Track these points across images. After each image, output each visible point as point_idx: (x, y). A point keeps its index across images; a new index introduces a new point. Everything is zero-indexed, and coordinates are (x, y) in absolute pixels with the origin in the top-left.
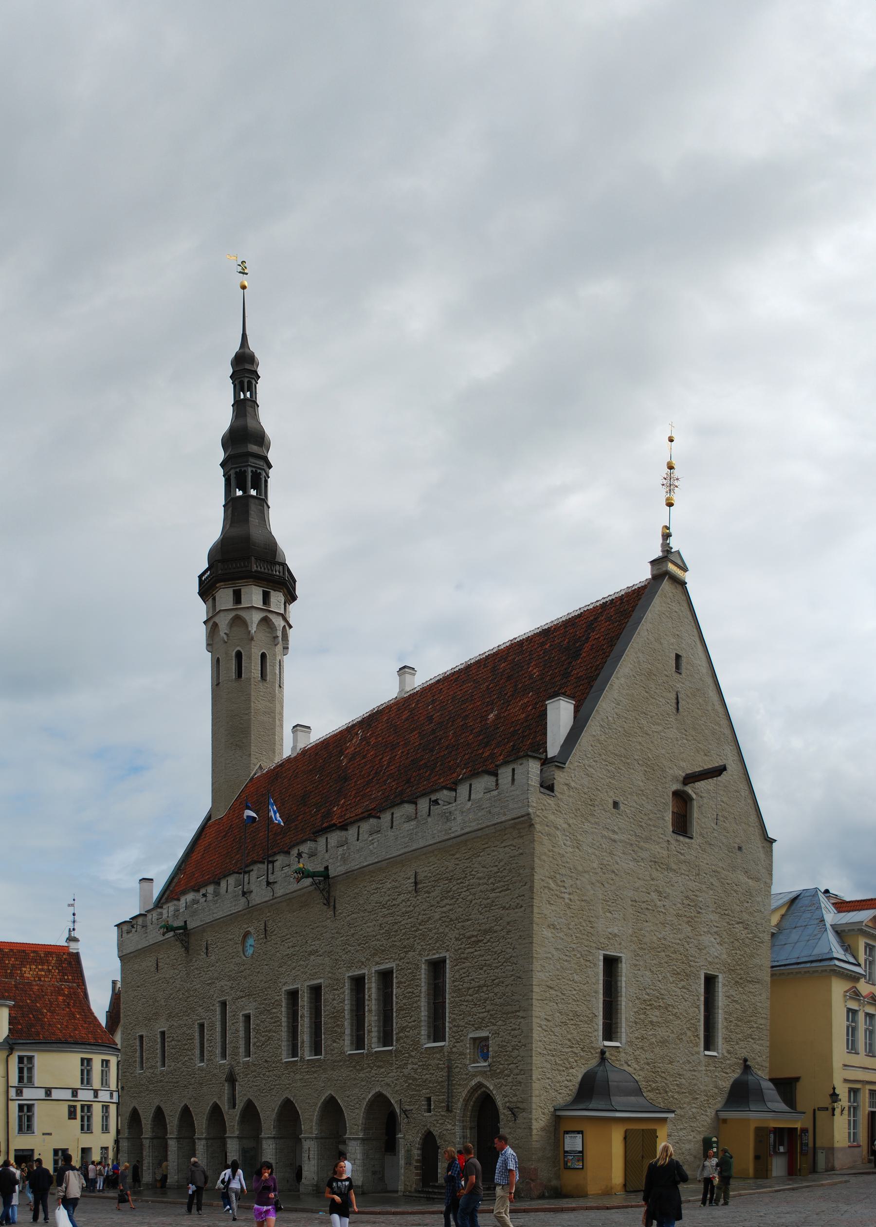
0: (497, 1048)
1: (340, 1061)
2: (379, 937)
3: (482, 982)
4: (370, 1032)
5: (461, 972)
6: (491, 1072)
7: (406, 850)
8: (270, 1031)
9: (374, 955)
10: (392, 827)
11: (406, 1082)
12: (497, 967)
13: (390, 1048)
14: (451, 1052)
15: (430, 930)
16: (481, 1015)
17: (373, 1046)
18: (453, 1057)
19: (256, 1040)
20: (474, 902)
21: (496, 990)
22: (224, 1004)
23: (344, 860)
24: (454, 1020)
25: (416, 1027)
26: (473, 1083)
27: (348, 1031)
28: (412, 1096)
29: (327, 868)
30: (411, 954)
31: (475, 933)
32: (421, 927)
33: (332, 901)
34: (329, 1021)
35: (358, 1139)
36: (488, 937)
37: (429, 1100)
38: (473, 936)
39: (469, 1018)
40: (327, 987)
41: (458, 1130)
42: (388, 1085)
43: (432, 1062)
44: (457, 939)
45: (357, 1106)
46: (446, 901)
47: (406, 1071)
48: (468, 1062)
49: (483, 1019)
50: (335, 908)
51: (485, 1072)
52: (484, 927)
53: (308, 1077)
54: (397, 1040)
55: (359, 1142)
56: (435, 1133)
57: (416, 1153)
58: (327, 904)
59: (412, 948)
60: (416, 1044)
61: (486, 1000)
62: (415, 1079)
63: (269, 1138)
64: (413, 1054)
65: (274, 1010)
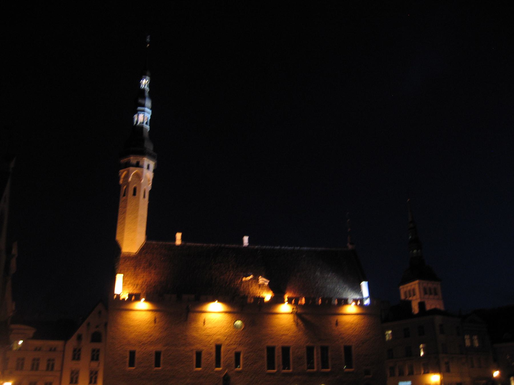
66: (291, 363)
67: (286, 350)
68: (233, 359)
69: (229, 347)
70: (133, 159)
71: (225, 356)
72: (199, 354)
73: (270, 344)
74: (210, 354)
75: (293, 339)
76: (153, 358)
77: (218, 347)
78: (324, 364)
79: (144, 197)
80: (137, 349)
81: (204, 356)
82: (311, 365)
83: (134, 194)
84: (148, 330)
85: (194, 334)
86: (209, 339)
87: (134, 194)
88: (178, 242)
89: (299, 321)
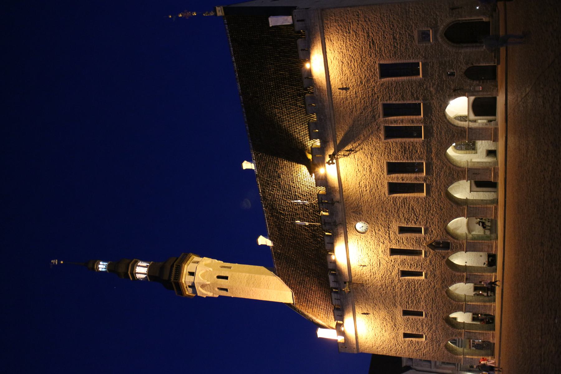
1: (427, 146)
5: (386, 52)
12: (385, 27)
14: (425, 58)
21: (396, 26)
24: (409, 56)
25: (412, 85)
26: (440, 40)
28: (446, 86)
38: (370, 45)
40: (388, 157)
41: (463, 51)
44: (371, 56)
47: (434, 92)
48: (430, 44)
49: (409, 35)
52: (366, 38)
54: (418, 99)
56: (465, 68)
60: (421, 84)
61: (400, 33)
62: (438, 86)
64: (425, 86)
67: (392, 168)
68: (408, 235)
70: (189, 292)
71: (406, 242)
72: (404, 273)
73: (386, 189)
74: (403, 262)
75: (375, 158)
76: (411, 317)
77: (393, 252)
78: (414, 110)
79: (226, 278)
80: (401, 332)
81: (407, 269)
83: (226, 290)
84: (378, 320)
85: (378, 276)
86: (383, 262)
87: (226, 290)
88: (269, 243)
89: (349, 147)
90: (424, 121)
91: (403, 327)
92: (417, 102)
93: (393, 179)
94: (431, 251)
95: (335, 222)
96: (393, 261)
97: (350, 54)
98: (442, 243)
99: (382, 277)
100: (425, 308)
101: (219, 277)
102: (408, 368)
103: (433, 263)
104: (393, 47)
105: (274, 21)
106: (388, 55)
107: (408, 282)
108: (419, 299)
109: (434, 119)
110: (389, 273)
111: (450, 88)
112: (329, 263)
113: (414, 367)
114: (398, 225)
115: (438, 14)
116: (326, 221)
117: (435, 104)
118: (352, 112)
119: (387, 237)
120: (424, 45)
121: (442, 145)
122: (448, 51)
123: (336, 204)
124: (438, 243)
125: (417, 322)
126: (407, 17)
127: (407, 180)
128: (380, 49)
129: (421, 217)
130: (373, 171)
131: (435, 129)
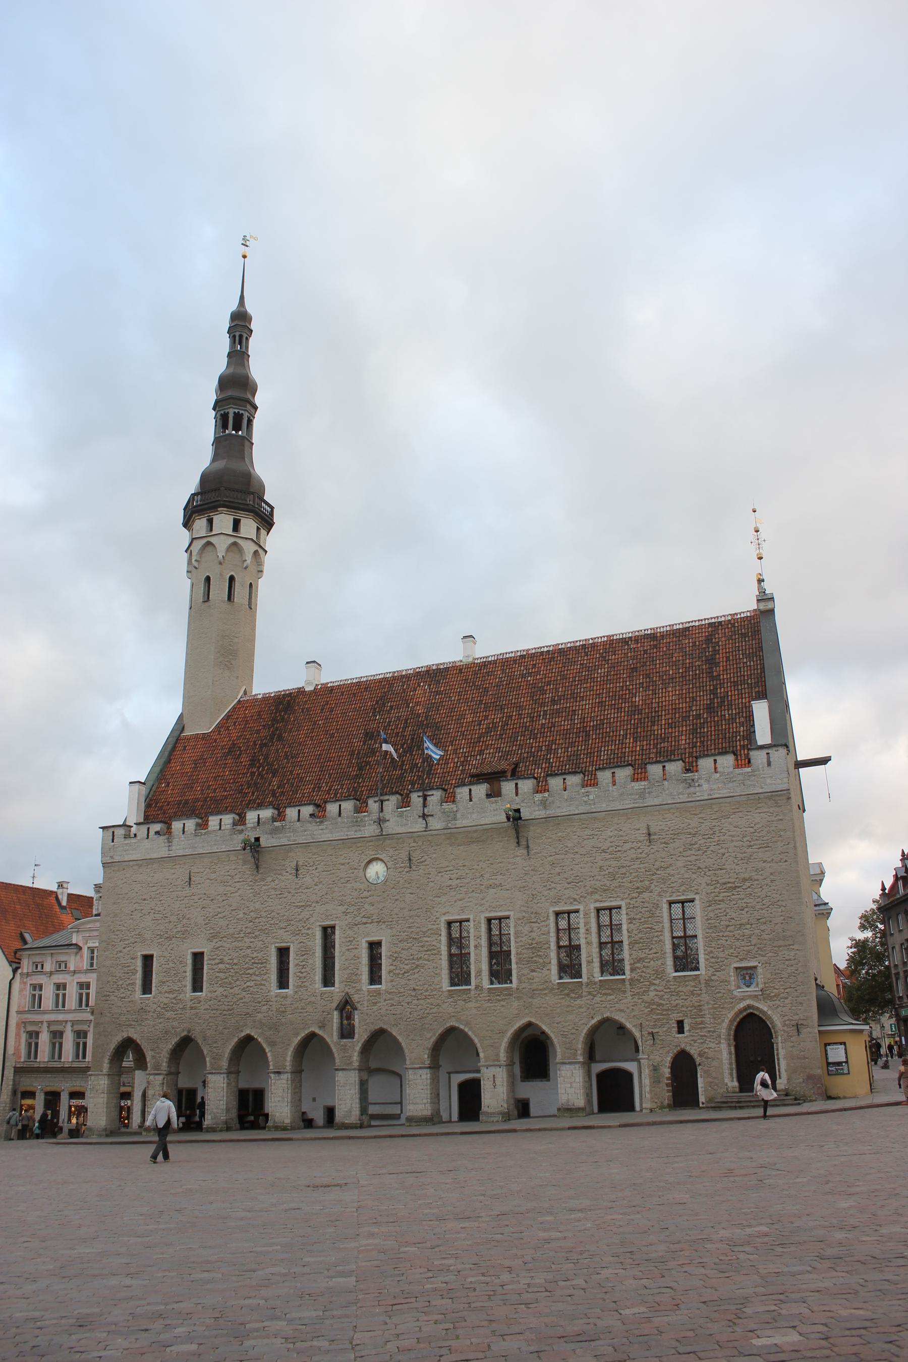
0: (769, 976)
1: (545, 989)
2: (599, 878)
3: (743, 921)
4: (590, 962)
5: (717, 912)
6: (764, 994)
7: (637, 805)
8: (418, 959)
9: (592, 893)
10: (614, 783)
11: (646, 1007)
12: (762, 909)
13: (624, 977)
14: (708, 981)
15: (673, 875)
16: (745, 948)
17: (595, 975)
18: (712, 984)
19: (392, 968)
20: (727, 855)
21: (763, 927)
22: (328, 932)
23: (544, 804)
24: (712, 952)
26: (742, 1005)
27: (554, 962)
29: (518, 811)
30: (646, 895)
31: (732, 880)
32: (658, 872)
33: (523, 842)
34: (525, 951)
35: (579, 1062)
36: (748, 884)
37: (680, 1024)
39: (731, 951)
40: (519, 919)
41: (724, 1046)
42: (622, 1011)
43: (683, 989)
44: (708, 885)
45: (574, 1031)
46: (689, 852)
48: (733, 988)
50: (528, 847)
51: (756, 996)
52: (743, 876)
53: (489, 1005)
54: (632, 970)
55: (577, 1066)
56: (694, 1051)
57: (667, 1072)
58: (518, 843)
59: (647, 889)
60: (660, 973)
62: (659, 1005)
63: (420, 1068)
64: (657, 982)
65: (425, 939)
66: (514, 966)
69: (350, 932)
82: (570, 966)
90: (590, 983)
91: (166, 954)
92: (627, 968)
93: (477, 928)
94: (335, 1005)
95: (385, 821)
96: (309, 932)
97: (711, 848)
98: (349, 1024)
99: (273, 911)
100: (209, 995)
101: (232, 579)
102: (15, 963)
103: (310, 1008)
104: (727, 923)
105: (761, 710)
106: (712, 915)
107: (264, 962)
108: (230, 984)
109: (597, 999)
110: (282, 925)
111: (654, 1026)
112: (297, 808)
113: (18, 976)
114: (384, 939)
115: (787, 1001)
116: (385, 803)
117: (625, 1001)
118: (604, 851)
119: (359, 919)
120: (733, 978)
121: (547, 1015)
122: (723, 1021)
123: (421, 819)
124: (349, 1017)
125: (179, 981)
126: (780, 946)
127: (476, 955)
128: (723, 901)
129: (403, 982)
130: (492, 891)
131: (578, 1002)
